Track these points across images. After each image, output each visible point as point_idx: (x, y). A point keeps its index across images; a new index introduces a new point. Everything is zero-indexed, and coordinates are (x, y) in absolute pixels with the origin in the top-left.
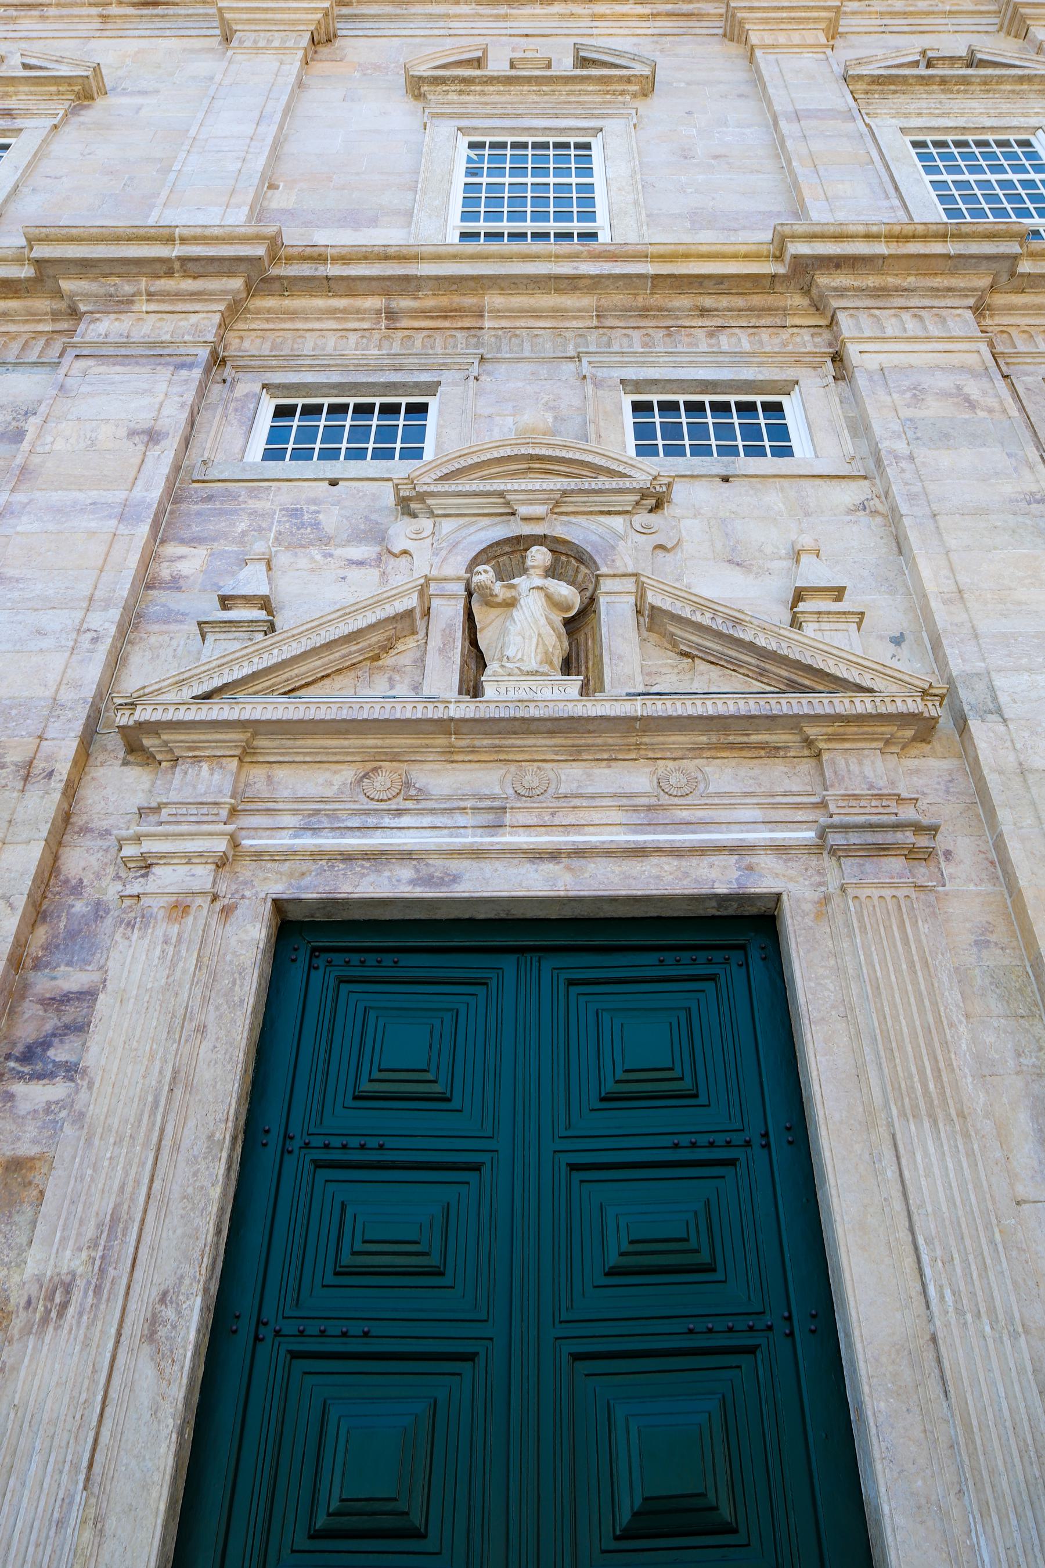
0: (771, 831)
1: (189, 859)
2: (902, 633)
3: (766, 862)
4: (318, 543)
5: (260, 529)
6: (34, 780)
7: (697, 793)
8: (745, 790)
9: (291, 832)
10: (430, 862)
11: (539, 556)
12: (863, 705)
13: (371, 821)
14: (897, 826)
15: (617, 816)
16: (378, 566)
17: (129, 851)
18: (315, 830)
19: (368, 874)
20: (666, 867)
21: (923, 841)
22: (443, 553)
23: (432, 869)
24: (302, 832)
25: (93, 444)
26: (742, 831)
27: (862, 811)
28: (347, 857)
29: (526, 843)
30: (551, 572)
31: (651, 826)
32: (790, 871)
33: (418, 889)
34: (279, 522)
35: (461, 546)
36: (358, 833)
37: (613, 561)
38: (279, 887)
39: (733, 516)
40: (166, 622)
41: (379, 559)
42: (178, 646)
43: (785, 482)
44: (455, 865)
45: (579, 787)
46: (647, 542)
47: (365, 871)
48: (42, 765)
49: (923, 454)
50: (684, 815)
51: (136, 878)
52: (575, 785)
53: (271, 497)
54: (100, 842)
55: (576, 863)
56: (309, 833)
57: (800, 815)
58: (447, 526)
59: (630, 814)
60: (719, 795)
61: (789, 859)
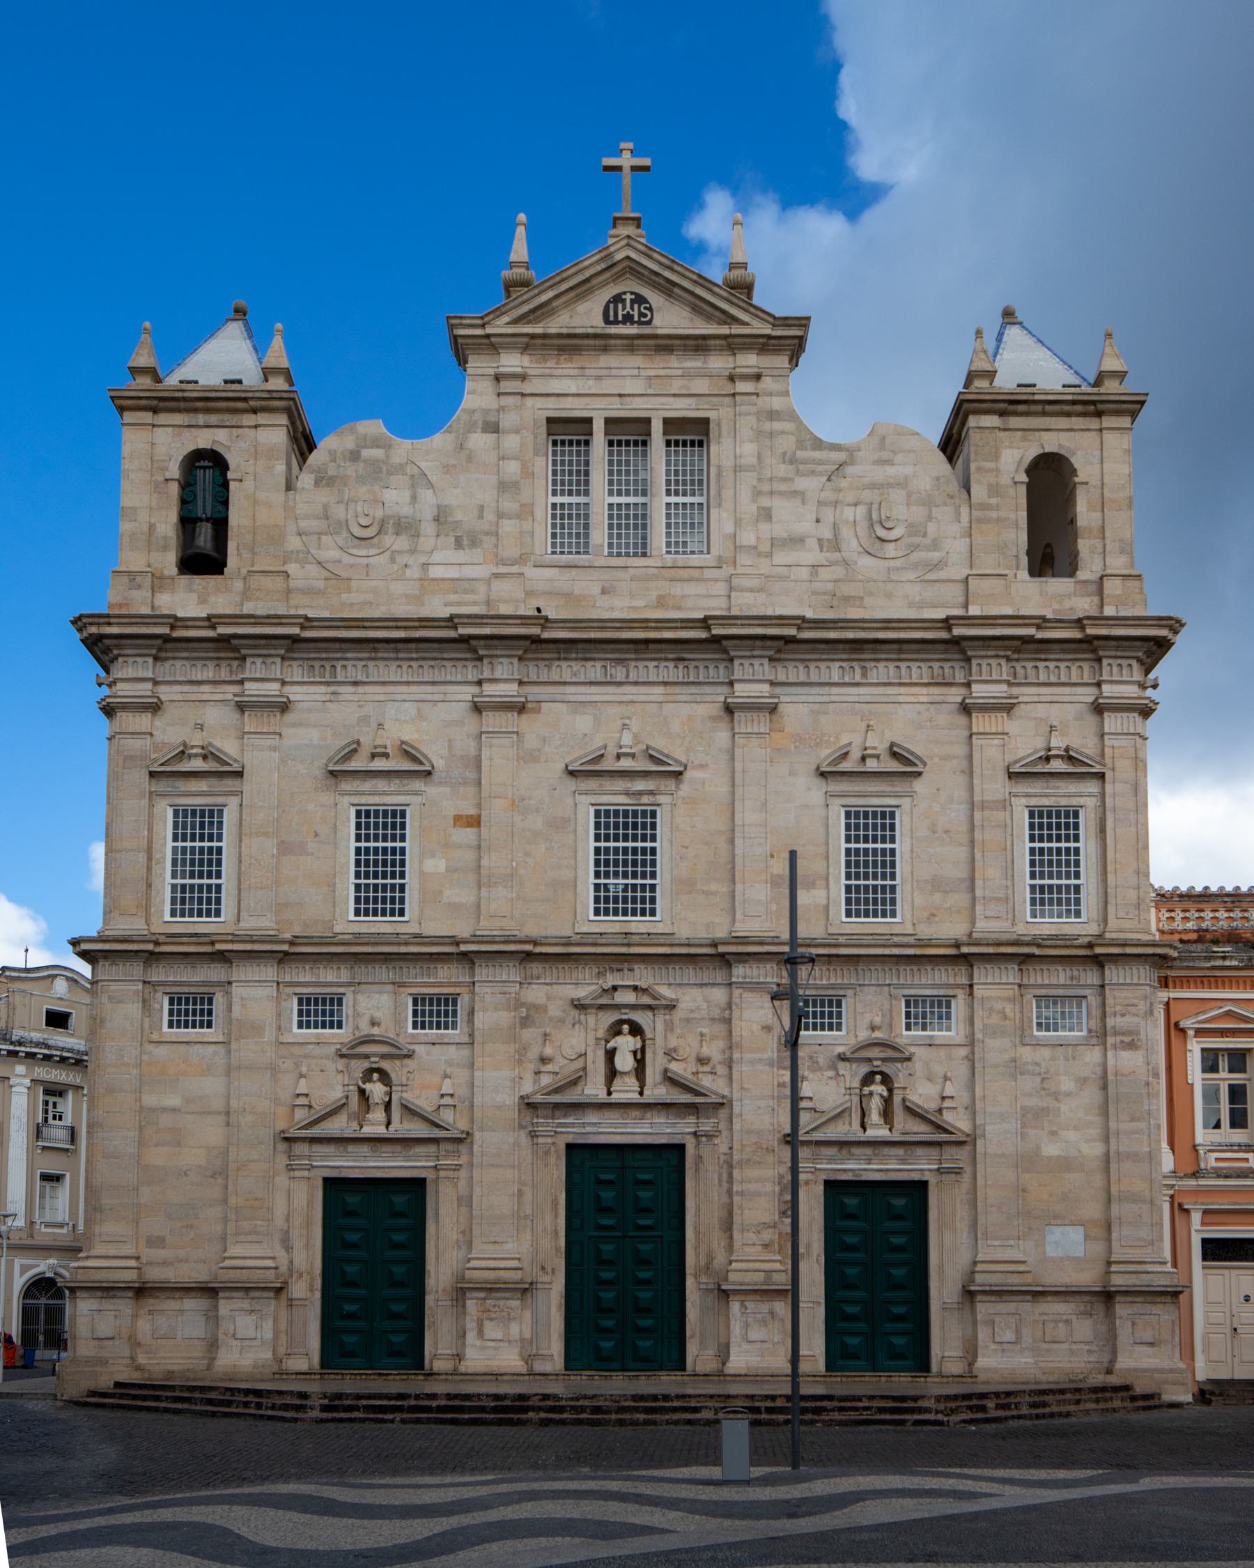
3: (927, 1173)
11: (878, 1077)
12: (952, 1138)
30: (883, 1082)
38: (825, 1177)
46: (906, 1073)
58: (854, 1066)
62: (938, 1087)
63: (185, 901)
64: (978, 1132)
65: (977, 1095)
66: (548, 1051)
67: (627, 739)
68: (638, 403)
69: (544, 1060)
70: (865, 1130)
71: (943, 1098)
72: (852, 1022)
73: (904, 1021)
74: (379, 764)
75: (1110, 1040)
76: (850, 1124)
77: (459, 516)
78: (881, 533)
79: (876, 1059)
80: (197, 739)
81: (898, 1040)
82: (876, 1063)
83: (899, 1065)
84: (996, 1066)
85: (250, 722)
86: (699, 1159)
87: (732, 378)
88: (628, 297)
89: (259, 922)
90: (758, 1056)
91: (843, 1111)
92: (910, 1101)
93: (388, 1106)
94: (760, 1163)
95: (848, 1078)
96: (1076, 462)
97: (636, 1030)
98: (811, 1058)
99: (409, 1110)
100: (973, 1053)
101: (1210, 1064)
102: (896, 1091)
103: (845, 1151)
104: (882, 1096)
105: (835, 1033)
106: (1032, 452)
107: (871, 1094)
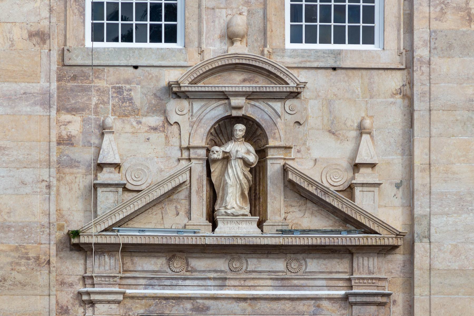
0: (329, 290)
1: (109, 302)
2: (401, 181)
4: (133, 114)
5: (104, 103)
6: (42, 265)
7: (302, 271)
8: (321, 271)
9: (143, 286)
10: (198, 301)
11: (240, 129)
12: (371, 240)
13: (174, 282)
14: (375, 295)
15: (269, 282)
16: (164, 131)
17: (85, 298)
18: (152, 286)
19: (175, 306)
20: (287, 305)
21: (384, 300)
22: (195, 126)
23: (199, 304)
24: (147, 287)
25: (12, 45)
26: (317, 290)
27: (364, 285)
28: (167, 298)
29: (234, 294)
31: (283, 287)
32: (333, 308)
33: (194, 313)
34: (112, 97)
35: (203, 121)
36: (169, 288)
37: (275, 134)
39: (335, 97)
40: (71, 167)
41: (164, 126)
42: (80, 183)
43: (364, 72)
44: (207, 302)
45: (255, 268)
46: (291, 119)
47: (174, 305)
48: (44, 257)
49: (435, 60)
50: (296, 282)
51: (89, 307)
52: (254, 267)
53: (105, 78)
54: (70, 289)
55: (254, 302)
56: (151, 287)
57: (341, 283)
58: (197, 105)
59: (274, 281)
60: (310, 272)
61: (334, 303)
62: (349, 146)
64: (416, 228)
65: (417, 162)
70: (214, 226)
71: (356, 167)
72: (193, 25)
73: (288, 23)
76: (189, 214)
79: (237, 94)
81: (277, 60)
82: (235, 101)
83: (277, 105)
84: (453, 108)
90: (21, 87)
91: (175, 190)
92: (296, 172)
94: (23, 285)
95: (185, 129)
98: (119, 90)
100: (411, 83)
102: (271, 154)
103: (178, 264)
104: (246, 163)
105: (163, 45)
107: (227, 158)
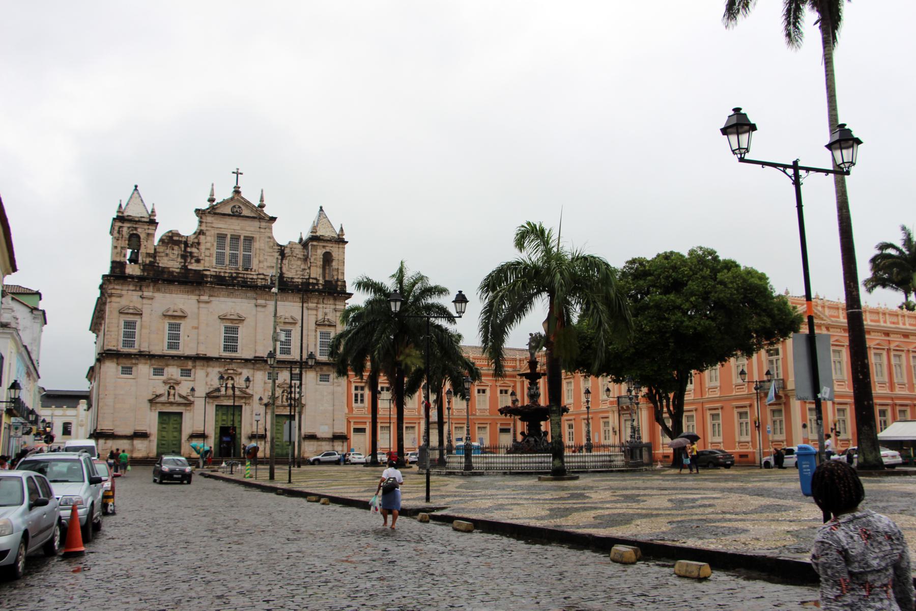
63: (126, 344)
66: (212, 383)
67: (233, 311)
68: (240, 232)
69: (211, 385)
74: (175, 314)
75: (335, 384)
77: (195, 255)
78: (290, 266)
80: (132, 305)
85: (145, 301)
86: (245, 409)
87: (260, 228)
88: (237, 206)
89: (145, 348)
93: (174, 395)
96: (333, 254)
97: (232, 379)
99: (181, 396)
101: (356, 388)
106: (324, 251)
